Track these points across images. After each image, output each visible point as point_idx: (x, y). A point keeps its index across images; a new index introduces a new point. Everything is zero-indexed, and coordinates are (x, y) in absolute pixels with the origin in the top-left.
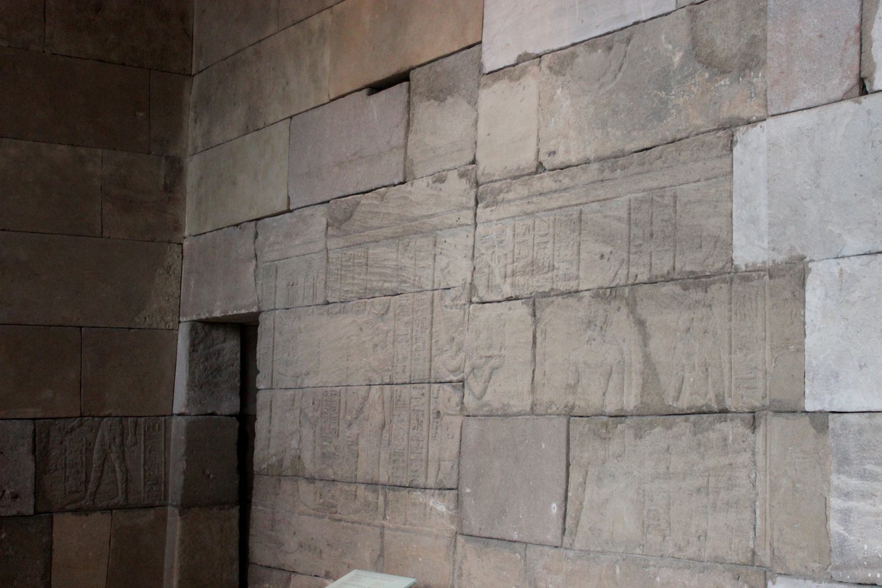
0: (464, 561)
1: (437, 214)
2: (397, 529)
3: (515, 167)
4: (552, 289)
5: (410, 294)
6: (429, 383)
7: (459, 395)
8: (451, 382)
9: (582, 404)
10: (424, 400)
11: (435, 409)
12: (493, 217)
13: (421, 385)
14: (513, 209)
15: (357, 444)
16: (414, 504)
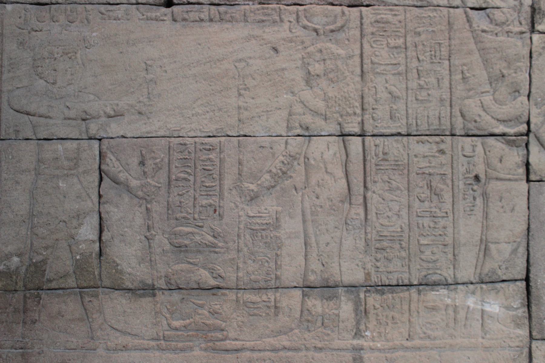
2: (394, 349)
6: (453, 135)
7: (520, 153)
8: (504, 135)
11: (468, 172)
13: (437, 139)
16: (434, 309)
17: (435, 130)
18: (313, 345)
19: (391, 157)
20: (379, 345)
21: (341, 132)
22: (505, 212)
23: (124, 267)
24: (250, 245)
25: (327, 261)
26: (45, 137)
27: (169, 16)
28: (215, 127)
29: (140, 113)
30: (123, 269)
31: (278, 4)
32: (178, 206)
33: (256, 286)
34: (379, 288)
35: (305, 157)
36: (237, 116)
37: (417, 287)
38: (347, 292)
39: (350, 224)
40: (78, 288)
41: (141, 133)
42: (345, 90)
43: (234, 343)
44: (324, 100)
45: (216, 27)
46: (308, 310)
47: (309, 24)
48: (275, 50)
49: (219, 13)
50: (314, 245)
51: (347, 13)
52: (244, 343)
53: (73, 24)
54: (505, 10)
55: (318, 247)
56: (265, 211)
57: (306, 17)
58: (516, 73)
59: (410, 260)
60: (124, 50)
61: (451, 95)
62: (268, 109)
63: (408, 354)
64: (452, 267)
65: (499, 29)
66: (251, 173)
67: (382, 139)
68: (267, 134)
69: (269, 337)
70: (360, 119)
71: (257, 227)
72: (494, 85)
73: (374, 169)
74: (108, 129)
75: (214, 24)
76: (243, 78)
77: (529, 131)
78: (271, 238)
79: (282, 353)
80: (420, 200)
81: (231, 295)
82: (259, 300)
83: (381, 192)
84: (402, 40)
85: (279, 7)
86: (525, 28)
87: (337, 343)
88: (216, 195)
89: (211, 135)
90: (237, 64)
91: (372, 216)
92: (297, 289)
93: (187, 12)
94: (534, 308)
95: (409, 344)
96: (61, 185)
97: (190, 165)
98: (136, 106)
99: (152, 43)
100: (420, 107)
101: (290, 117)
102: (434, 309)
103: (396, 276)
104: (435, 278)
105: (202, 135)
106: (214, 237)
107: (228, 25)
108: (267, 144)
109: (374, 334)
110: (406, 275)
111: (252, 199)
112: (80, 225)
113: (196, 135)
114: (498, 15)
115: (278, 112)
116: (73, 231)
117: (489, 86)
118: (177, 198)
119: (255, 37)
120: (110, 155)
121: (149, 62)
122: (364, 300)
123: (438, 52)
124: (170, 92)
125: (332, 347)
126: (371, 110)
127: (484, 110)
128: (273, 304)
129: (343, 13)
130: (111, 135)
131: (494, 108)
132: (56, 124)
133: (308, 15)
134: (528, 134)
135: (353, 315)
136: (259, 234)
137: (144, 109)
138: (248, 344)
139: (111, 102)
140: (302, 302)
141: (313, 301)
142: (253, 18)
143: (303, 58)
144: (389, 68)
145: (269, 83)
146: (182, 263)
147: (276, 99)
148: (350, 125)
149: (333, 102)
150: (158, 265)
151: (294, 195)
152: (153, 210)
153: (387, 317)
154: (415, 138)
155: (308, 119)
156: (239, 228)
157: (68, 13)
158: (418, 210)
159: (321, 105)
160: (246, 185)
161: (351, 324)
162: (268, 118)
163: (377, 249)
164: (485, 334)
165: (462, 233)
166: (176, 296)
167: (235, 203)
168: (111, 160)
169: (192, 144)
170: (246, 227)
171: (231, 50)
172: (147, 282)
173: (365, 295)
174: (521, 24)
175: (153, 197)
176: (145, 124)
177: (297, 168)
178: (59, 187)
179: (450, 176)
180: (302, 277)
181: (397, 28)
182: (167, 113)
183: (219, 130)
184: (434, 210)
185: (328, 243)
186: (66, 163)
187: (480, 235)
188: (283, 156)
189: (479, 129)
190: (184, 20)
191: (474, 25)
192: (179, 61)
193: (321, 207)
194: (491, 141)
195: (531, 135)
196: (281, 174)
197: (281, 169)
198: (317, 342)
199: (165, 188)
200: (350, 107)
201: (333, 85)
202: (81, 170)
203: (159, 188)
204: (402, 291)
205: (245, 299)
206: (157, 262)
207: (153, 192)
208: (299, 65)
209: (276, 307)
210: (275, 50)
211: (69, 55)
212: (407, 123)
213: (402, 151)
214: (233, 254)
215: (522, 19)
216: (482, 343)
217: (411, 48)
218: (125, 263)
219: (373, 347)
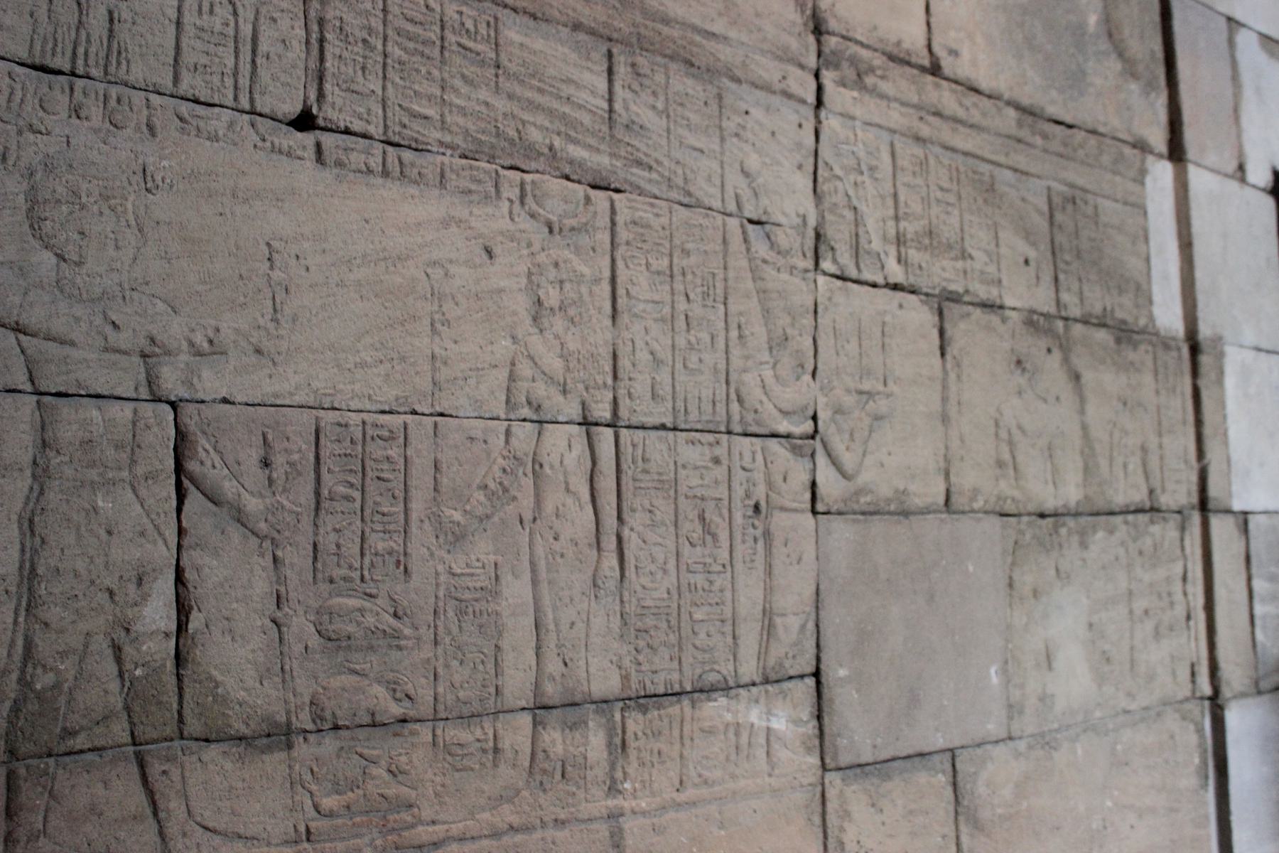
0: (846, 825)
1: (725, 38)
3: (894, 39)
4: (967, 292)
5: (663, 203)
8: (788, 436)
9: (1016, 493)
10: (720, 472)
11: (748, 496)
12: (858, 111)
13: (710, 438)
14: (896, 117)
15: (496, 594)
16: (710, 732)
17: (708, 422)
18: (553, 817)
19: (653, 467)
20: (644, 805)
21: (585, 417)
22: (791, 564)
23: (230, 690)
24: (455, 630)
25: (571, 655)
26: (62, 389)
27: (310, 153)
28: (394, 393)
29: (258, 351)
30: (228, 693)
31: (489, 162)
32: (334, 554)
33: (466, 711)
34: (642, 701)
35: (534, 461)
36: (429, 374)
37: (690, 695)
38: (596, 712)
39: (602, 586)
40: (134, 744)
41: (263, 395)
42: (592, 340)
43: (430, 829)
44: (561, 356)
45: (391, 191)
46: (544, 751)
47: (541, 211)
48: (489, 252)
49: (401, 162)
50: (552, 627)
51: (593, 198)
52: (446, 827)
53: (120, 132)
54: (789, 231)
55: (558, 631)
56: (477, 564)
57: (534, 196)
58: (801, 335)
59: (681, 649)
60: (227, 210)
61: (728, 364)
62: (480, 366)
63: (682, 815)
64: (731, 658)
65: (781, 261)
66: (454, 490)
67: (640, 433)
68: (476, 414)
69: (483, 810)
70: (611, 396)
71: (467, 595)
72: (775, 352)
73: (631, 488)
74: (195, 380)
75: (389, 183)
76: (440, 299)
77: (816, 431)
78: (489, 615)
79: (507, 840)
80: (690, 543)
81: (425, 732)
82: (470, 738)
83: (641, 528)
84: (666, 262)
85: (497, 172)
86: (810, 264)
87: (586, 809)
88: (400, 532)
89: (387, 408)
90: (429, 271)
91: (630, 572)
92: (526, 711)
93: (345, 150)
94: (826, 720)
95: (681, 797)
96: (100, 503)
97: (353, 467)
98: (252, 336)
99: (280, 204)
100: (690, 381)
101: (513, 384)
102: (710, 732)
103: (663, 679)
104: (712, 678)
105: (374, 408)
106: (395, 615)
107: (413, 190)
108: (478, 434)
109: (637, 785)
110: (675, 676)
111: (457, 540)
112: (145, 597)
113: (363, 408)
114: (782, 238)
115: (494, 371)
116: (129, 613)
117: (767, 353)
118: (333, 537)
119: (459, 222)
120: (203, 441)
121: (275, 244)
122: (620, 724)
123: (712, 288)
124: (314, 312)
125: (580, 816)
126: (627, 382)
127: (766, 393)
128: (491, 744)
129: (588, 200)
130: (200, 396)
131: (776, 389)
132: (85, 360)
133: (537, 192)
134: (813, 437)
135: (605, 755)
136: (470, 610)
137: (266, 345)
138: (456, 829)
139: (202, 321)
140: (533, 737)
141: (552, 732)
142: (454, 183)
143: (530, 274)
144: (649, 307)
145: (480, 314)
146: (340, 674)
147: (489, 348)
148: (600, 405)
149: (575, 362)
150: (298, 681)
151: (520, 533)
152: (287, 561)
153: (652, 751)
154: (684, 434)
155: (541, 390)
156: (436, 597)
157: (113, 103)
158: (689, 561)
159: (554, 364)
160: (449, 512)
161: (600, 772)
162: (478, 383)
163: (640, 631)
164: (773, 769)
165: (742, 599)
166: (330, 744)
167: (428, 549)
168: (206, 450)
169: (357, 425)
170: (449, 596)
171: (420, 240)
172: (278, 718)
173: (623, 717)
174: (804, 255)
175: (287, 534)
176: (270, 377)
177: (524, 481)
178: (95, 510)
179: (726, 503)
180: (533, 688)
181: (660, 238)
182: (310, 356)
183: (401, 401)
184: (708, 560)
185: (573, 624)
186: (110, 452)
187: (762, 603)
188: (504, 458)
189: (758, 423)
190: (339, 164)
191: (753, 250)
192: (331, 250)
193: (562, 556)
194: (773, 444)
195: (818, 438)
196: (501, 493)
197: (501, 484)
198: (558, 810)
199: (309, 516)
200: (599, 373)
201: (573, 329)
202: (140, 470)
203: (297, 514)
204: (672, 704)
205: (447, 739)
206: (295, 674)
207: (288, 524)
208: (523, 286)
209: (496, 750)
210: (489, 252)
211: (113, 202)
212: (674, 409)
213: (666, 455)
214: (427, 652)
215: (806, 248)
216: (770, 785)
217: (678, 278)
218: (232, 680)
219: (637, 809)
